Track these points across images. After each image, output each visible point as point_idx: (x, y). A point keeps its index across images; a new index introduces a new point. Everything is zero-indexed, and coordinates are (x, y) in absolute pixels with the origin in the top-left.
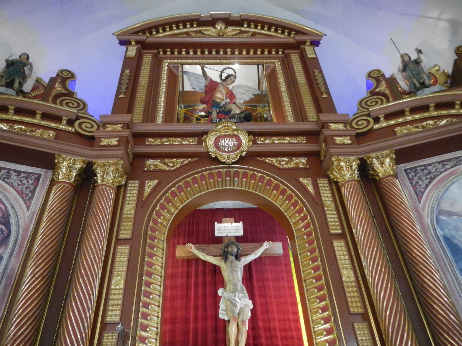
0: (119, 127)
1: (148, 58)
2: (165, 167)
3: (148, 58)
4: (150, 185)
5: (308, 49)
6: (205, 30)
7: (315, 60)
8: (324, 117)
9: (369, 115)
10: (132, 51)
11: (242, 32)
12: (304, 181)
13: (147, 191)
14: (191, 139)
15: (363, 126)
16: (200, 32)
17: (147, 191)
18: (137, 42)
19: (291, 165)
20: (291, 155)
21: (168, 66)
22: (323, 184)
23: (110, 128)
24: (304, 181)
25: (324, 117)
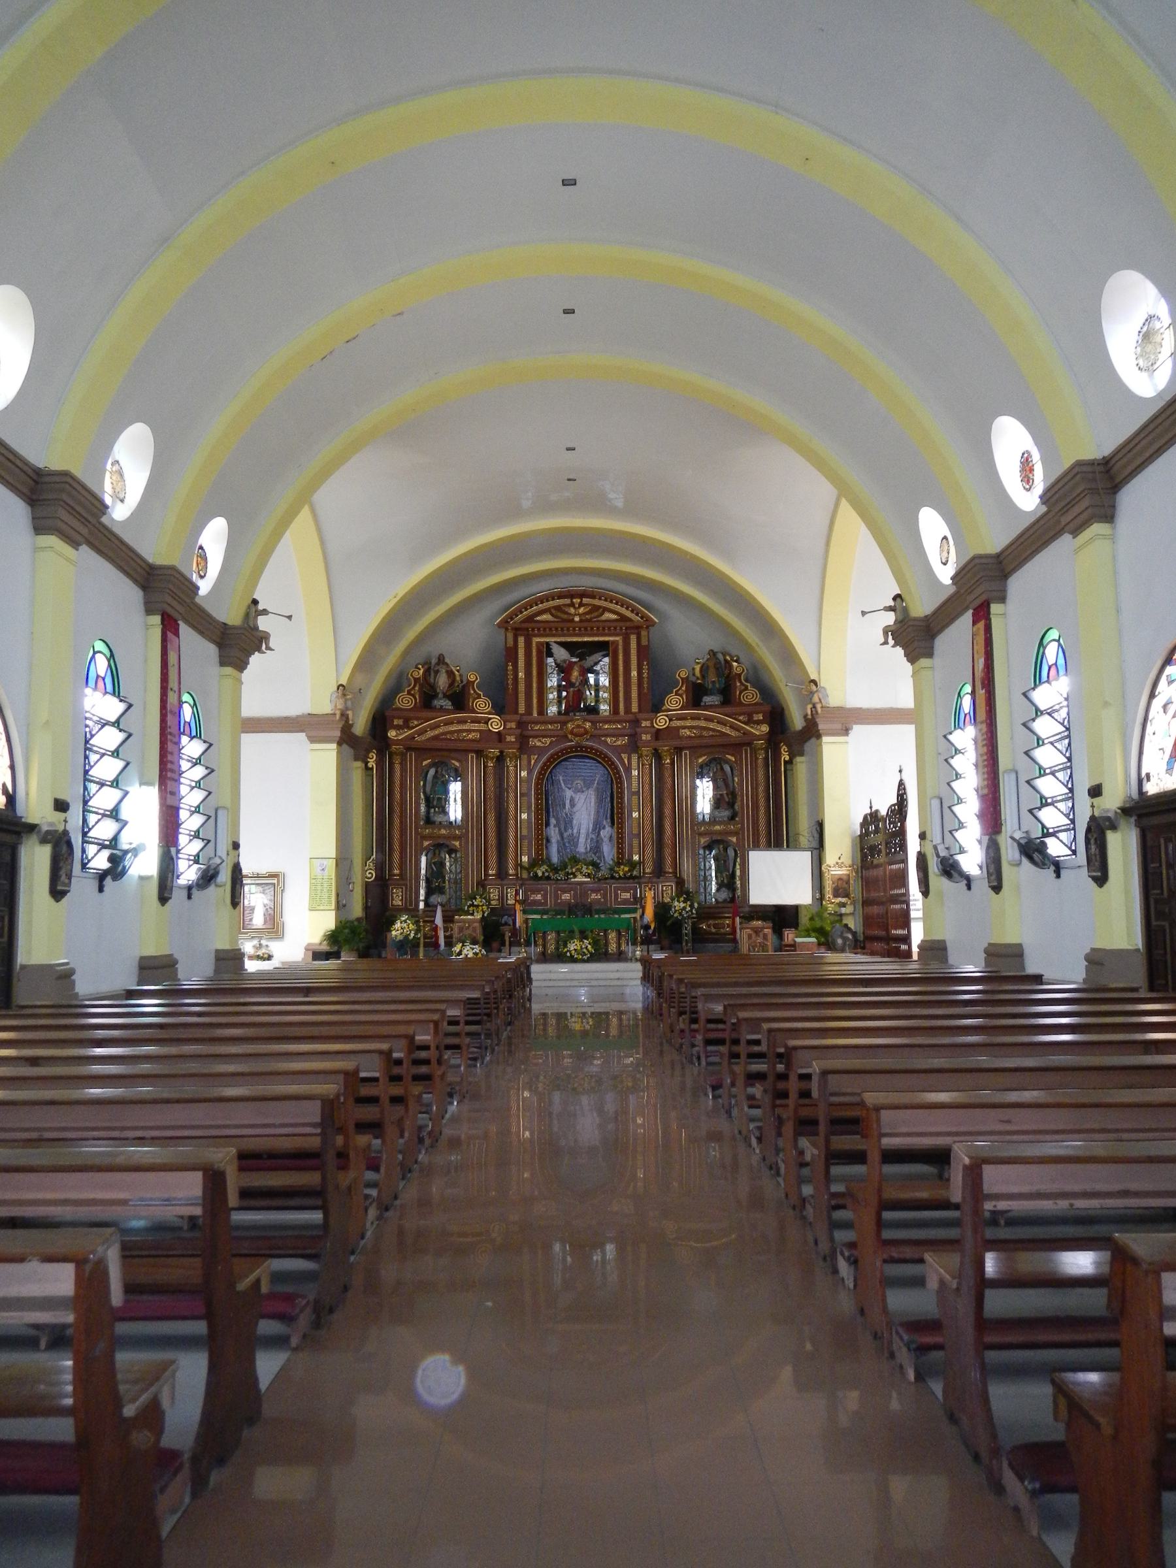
0: (513, 725)
1: (521, 640)
2: (538, 744)
3: (521, 640)
4: (534, 758)
5: (644, 633)
6: (565, 605)
7: (648, 647)
8: (640, 716)
9: (667, 716)
10: (510, 636)
11: (596, 608)
12: (623, 755)
13: (533, 762)
14: (556, 725)
15: (661, 722)
16: (558, 608)
17: (533, 762)
18: (512, 629)
19: (619, 743)
20: (617, 736)
21: (537, 645)
22: (634, 758)
23: (509, 725)
24: (623, 755)
25: (640, 716)
